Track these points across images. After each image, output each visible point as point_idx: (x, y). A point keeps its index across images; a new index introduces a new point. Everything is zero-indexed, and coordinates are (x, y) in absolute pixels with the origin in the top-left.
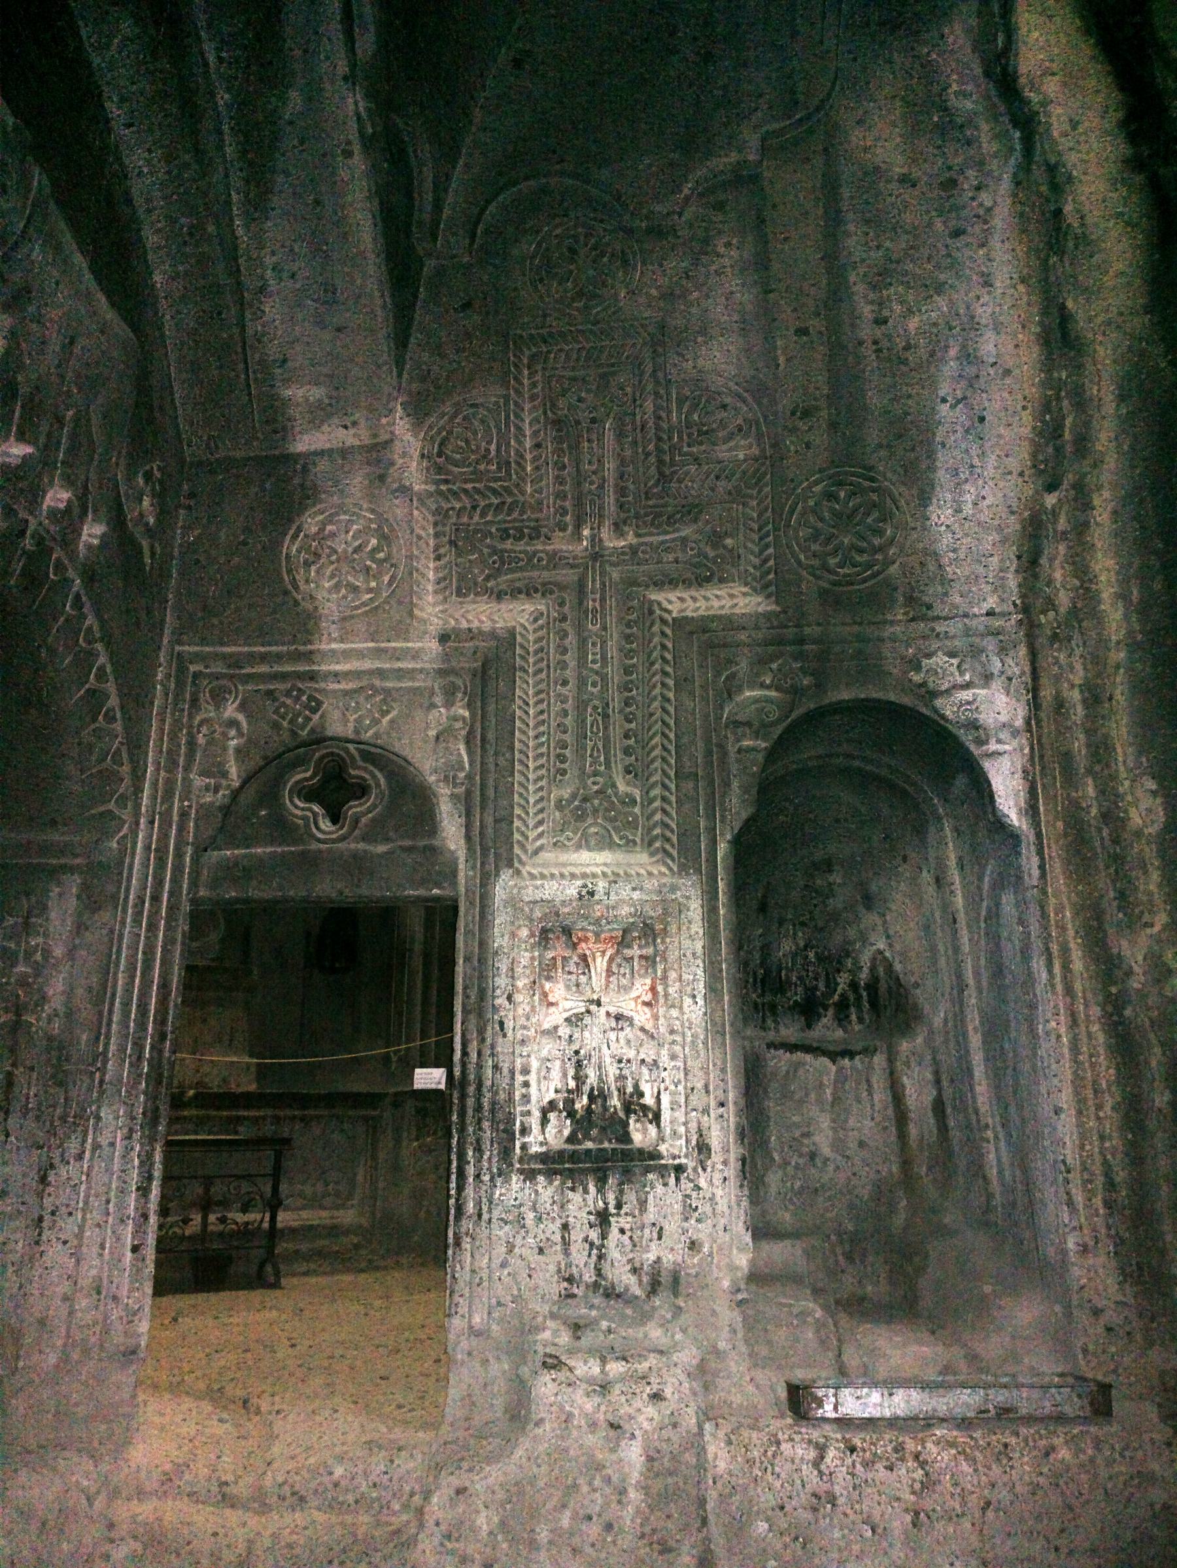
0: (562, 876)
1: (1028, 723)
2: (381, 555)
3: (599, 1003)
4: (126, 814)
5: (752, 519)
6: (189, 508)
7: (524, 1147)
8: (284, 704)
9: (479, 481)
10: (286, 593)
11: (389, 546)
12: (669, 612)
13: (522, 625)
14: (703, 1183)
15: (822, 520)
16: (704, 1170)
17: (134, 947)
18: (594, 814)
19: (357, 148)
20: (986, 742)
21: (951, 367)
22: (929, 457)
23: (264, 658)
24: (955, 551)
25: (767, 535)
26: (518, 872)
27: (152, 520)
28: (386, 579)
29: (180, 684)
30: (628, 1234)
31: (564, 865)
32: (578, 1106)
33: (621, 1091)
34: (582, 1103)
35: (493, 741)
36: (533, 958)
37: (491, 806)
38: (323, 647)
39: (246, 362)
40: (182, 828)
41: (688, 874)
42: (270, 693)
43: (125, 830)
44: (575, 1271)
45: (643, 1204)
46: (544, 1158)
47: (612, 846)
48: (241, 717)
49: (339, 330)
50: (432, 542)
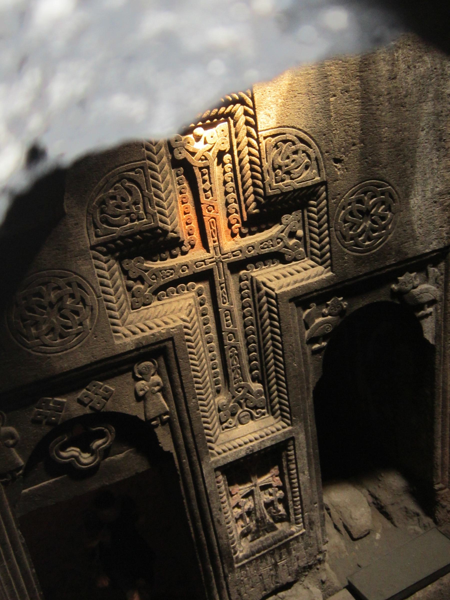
0: (235, 447)
1: (441, 299)
3: (255, 485)
5: (314, 220)
7: (237, 558)
12: (273, 290)
13: (184, 321)
14: (312, 535)
16: (312, 529)
18: (242, 408)
20: (423, 309)
21: (428, 107)
22: (412, 167)
24: (420, 219)
25: (324, 231)
26: (213, 455)
30: (286, 565)
32: (252, 526)
33: (269, 512)
34: (252, 525)
35: (182, 394)
37: (189, 427)
41: (297, 424)
44: (267, 587)
45: (289, 553)
46: (246, 557)
48: (12, 429)
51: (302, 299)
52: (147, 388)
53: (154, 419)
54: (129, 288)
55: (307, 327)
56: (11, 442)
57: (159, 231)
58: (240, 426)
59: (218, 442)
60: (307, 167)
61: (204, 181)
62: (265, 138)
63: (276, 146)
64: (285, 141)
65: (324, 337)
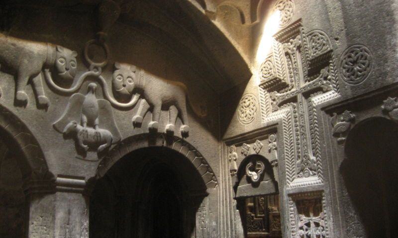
15: (348, 65)
17: (223, 211)
26: (288, 186)
31: (301, 182)
36: (294, 209)
40: (229, 183)
47: (309, 175)
51: (330, 109)
52: (271, 147)
53: (272, 162)
54: (272, 104)
55: (333, 126)
56: (235, 158)
57: (278, 79)
58: (304, 178)
59: (293, 182)
60: (324, 45)
61: (294, 59)
62: (308, 36)
63: (311, 39)
64: (315, 36)
65: (344, 134)
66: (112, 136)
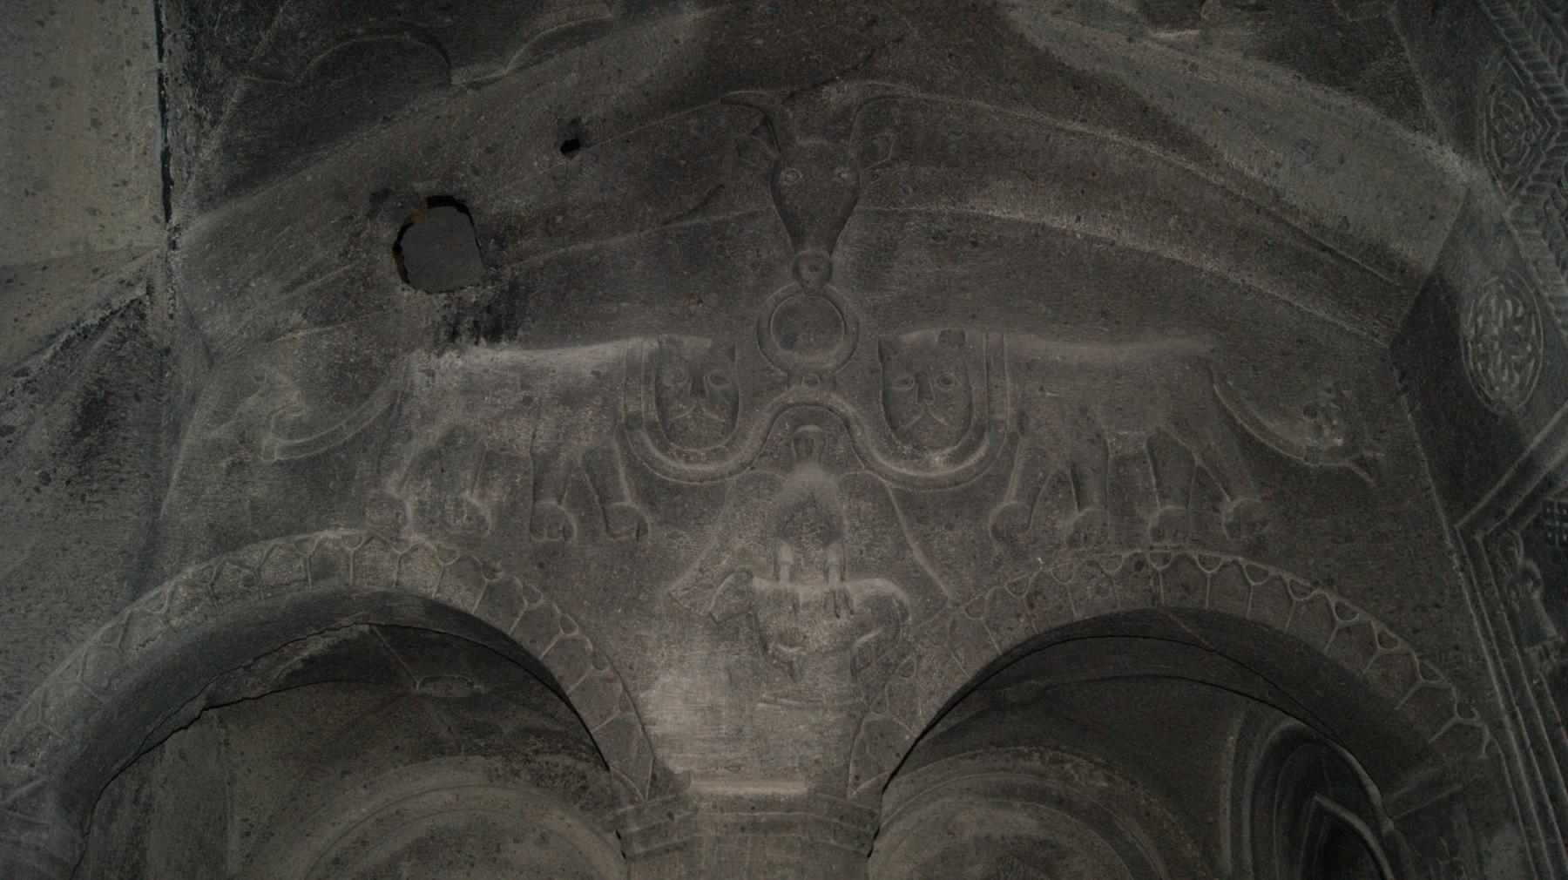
2: (1521, 310)
4: (1476, 720)
6: (1406, 389)
8: (1551, 529)
9: (1539, 156)
10: (1487, 413)
11: (1519, 297)
19: (1191, 60)
23: (1507, 493)
27: (1339, 442)
28: (1534, 331)
29: (1476, 559)
38: (1533, 446)
39: (1324, 249)
42: (1537, 523)
43: (1487, 735)
49: (1342, 161)
50: (1552, 257)
66: (902, 595)
